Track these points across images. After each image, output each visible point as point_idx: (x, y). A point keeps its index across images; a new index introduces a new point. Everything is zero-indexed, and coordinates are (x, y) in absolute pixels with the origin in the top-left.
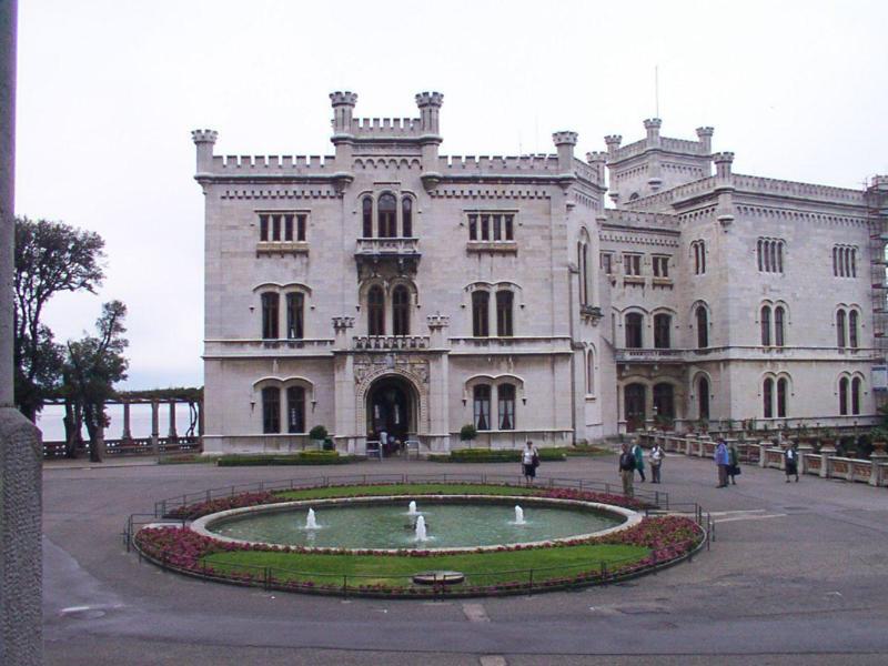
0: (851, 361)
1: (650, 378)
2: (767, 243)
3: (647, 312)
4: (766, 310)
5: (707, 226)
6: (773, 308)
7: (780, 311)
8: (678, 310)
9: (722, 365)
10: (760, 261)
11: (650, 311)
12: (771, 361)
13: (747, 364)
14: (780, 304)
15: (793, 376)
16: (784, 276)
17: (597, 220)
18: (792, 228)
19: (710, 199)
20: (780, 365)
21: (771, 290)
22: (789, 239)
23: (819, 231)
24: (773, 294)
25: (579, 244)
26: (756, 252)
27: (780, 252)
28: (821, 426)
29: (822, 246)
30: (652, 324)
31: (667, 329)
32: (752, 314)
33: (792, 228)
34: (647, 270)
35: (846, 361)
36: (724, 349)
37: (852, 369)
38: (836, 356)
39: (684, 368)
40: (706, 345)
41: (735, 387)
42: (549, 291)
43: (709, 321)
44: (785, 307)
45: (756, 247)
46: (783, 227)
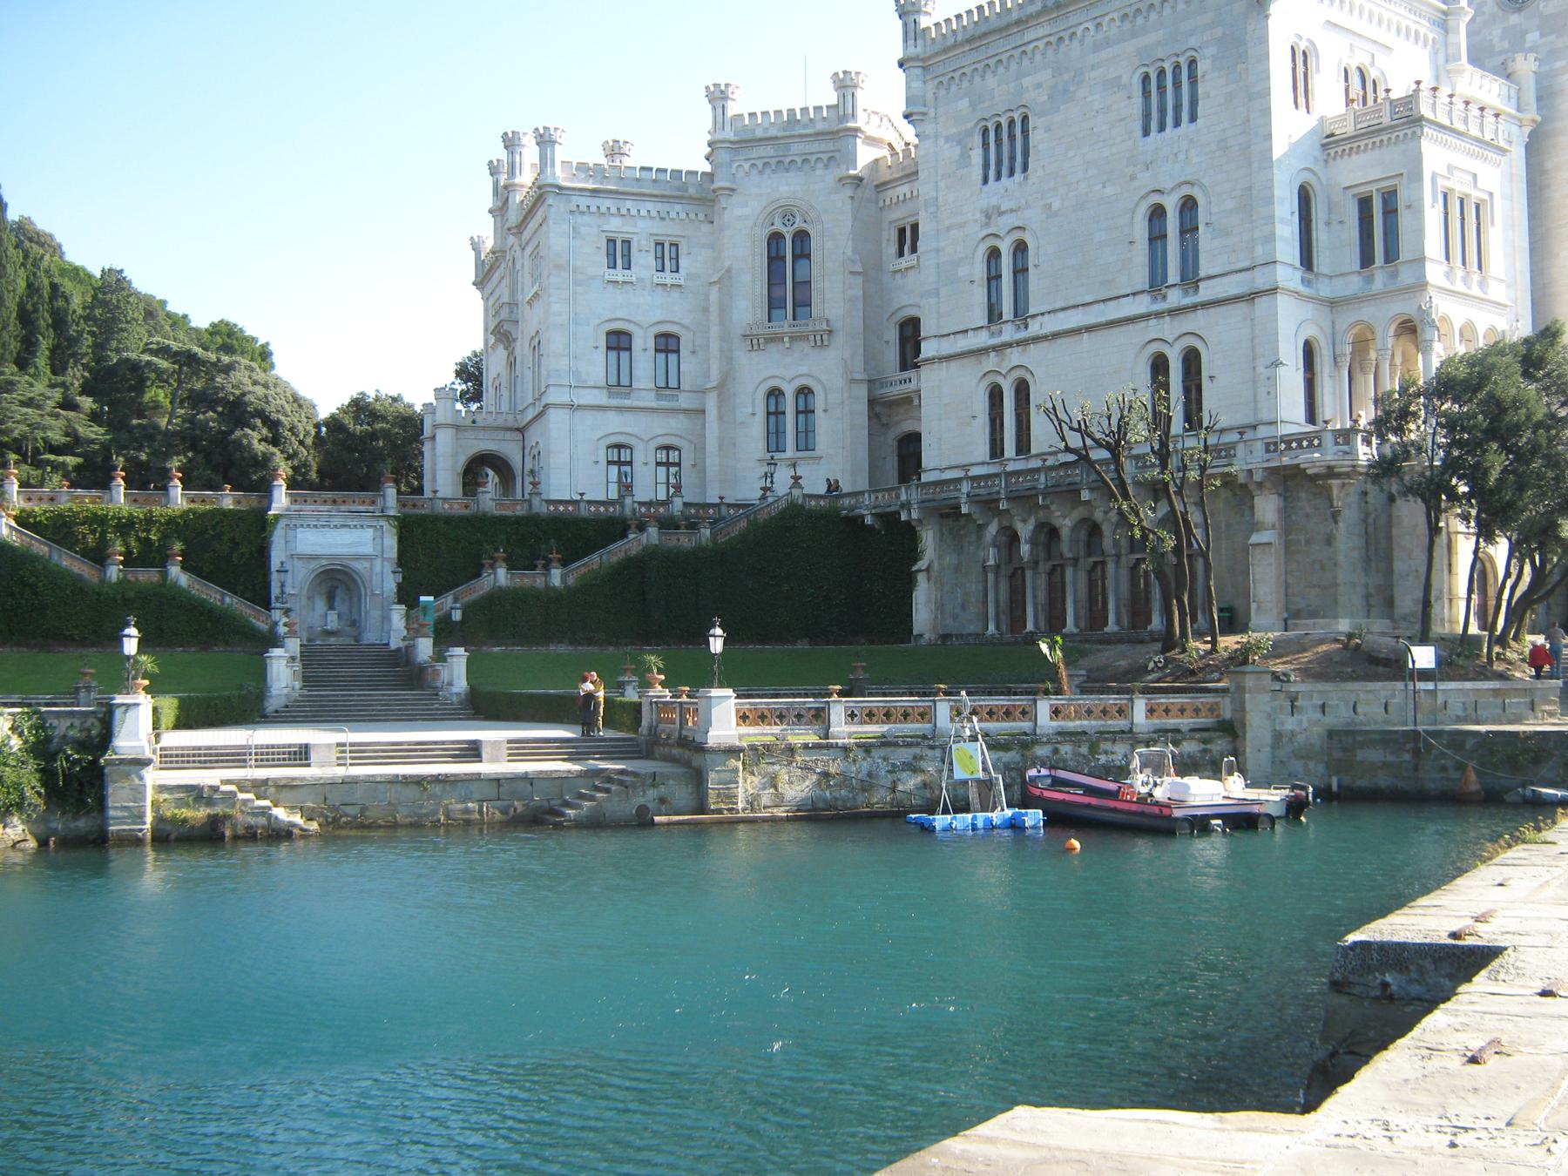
0: (1174, 312)
2: (998, 126)
7: (1021, 248)
10: (986, 166)
12: (995, 348)
13: (954, 365)
14: (1018, 235)
16: (1026, 178)
17: (840, 180)
18: (1045, 76)
21: (1001, 214)
23: (1105, 54)
24: (1005, 217)
25: (775, 239)
26: (977, 156)
27: (1025, 131)
28: (1048, 463)
29: (1115, 84)
32: (963, 272)
33: (1045, 76)
35: (1158, 315)
37: (1168, 329)
44: (1027, 237)
45: (978, 139)
46: (1026, 81)
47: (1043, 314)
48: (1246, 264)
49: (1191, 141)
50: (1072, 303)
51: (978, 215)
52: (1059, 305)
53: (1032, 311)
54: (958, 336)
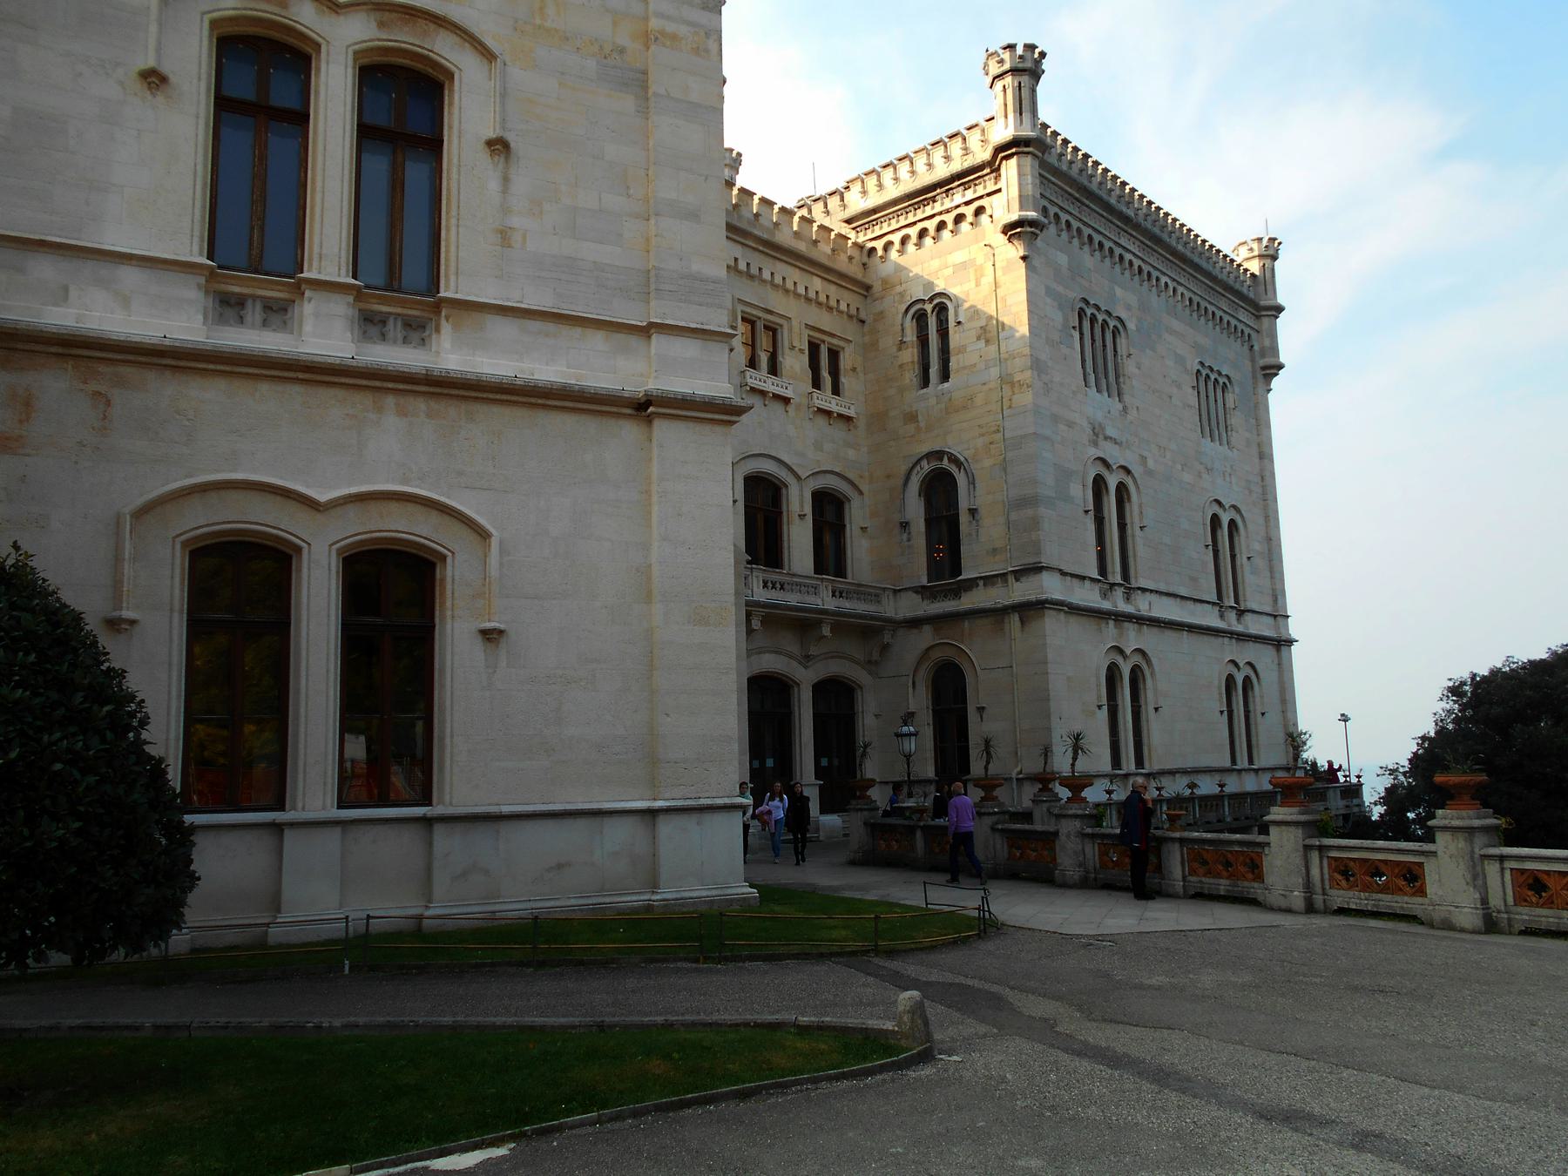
1: (806, 660)
2: (1093, 319)
3: (798, 477)
4: (1099, 484)
5: (958, 257)
6: (1112, 482)
8: (864, 487)
9: (1016, 617)
11: (803, 474)
12: (1120, 618)
15: (1154, 661)
16: (1125, 409)
18: (1132, 299)
19: (966, 186)
20: (1130, 628)
21: (1106, 438)
22: (1131, 326)
23: (1176, 324)
28: (1227, 790)
29: (1180, 360)
30: (808, 509)
31: (839, 529)
34: (795, 363)
36: (1019, 574)
38: (1210, 618)
39: (887, 638)
40: (956, 569)
41: (1057, 684)
42: (628, 103)
43: (964, 504)
44: (1129, 482)
46: (1119, 291)
47: (1151, 591)
48: (1268, 609)
49: (1232, 467)
50: (1171, 590)
51: (1085, 424)
52: (1163, 588)
53: (1143, 583)
54: (1075, 581)
